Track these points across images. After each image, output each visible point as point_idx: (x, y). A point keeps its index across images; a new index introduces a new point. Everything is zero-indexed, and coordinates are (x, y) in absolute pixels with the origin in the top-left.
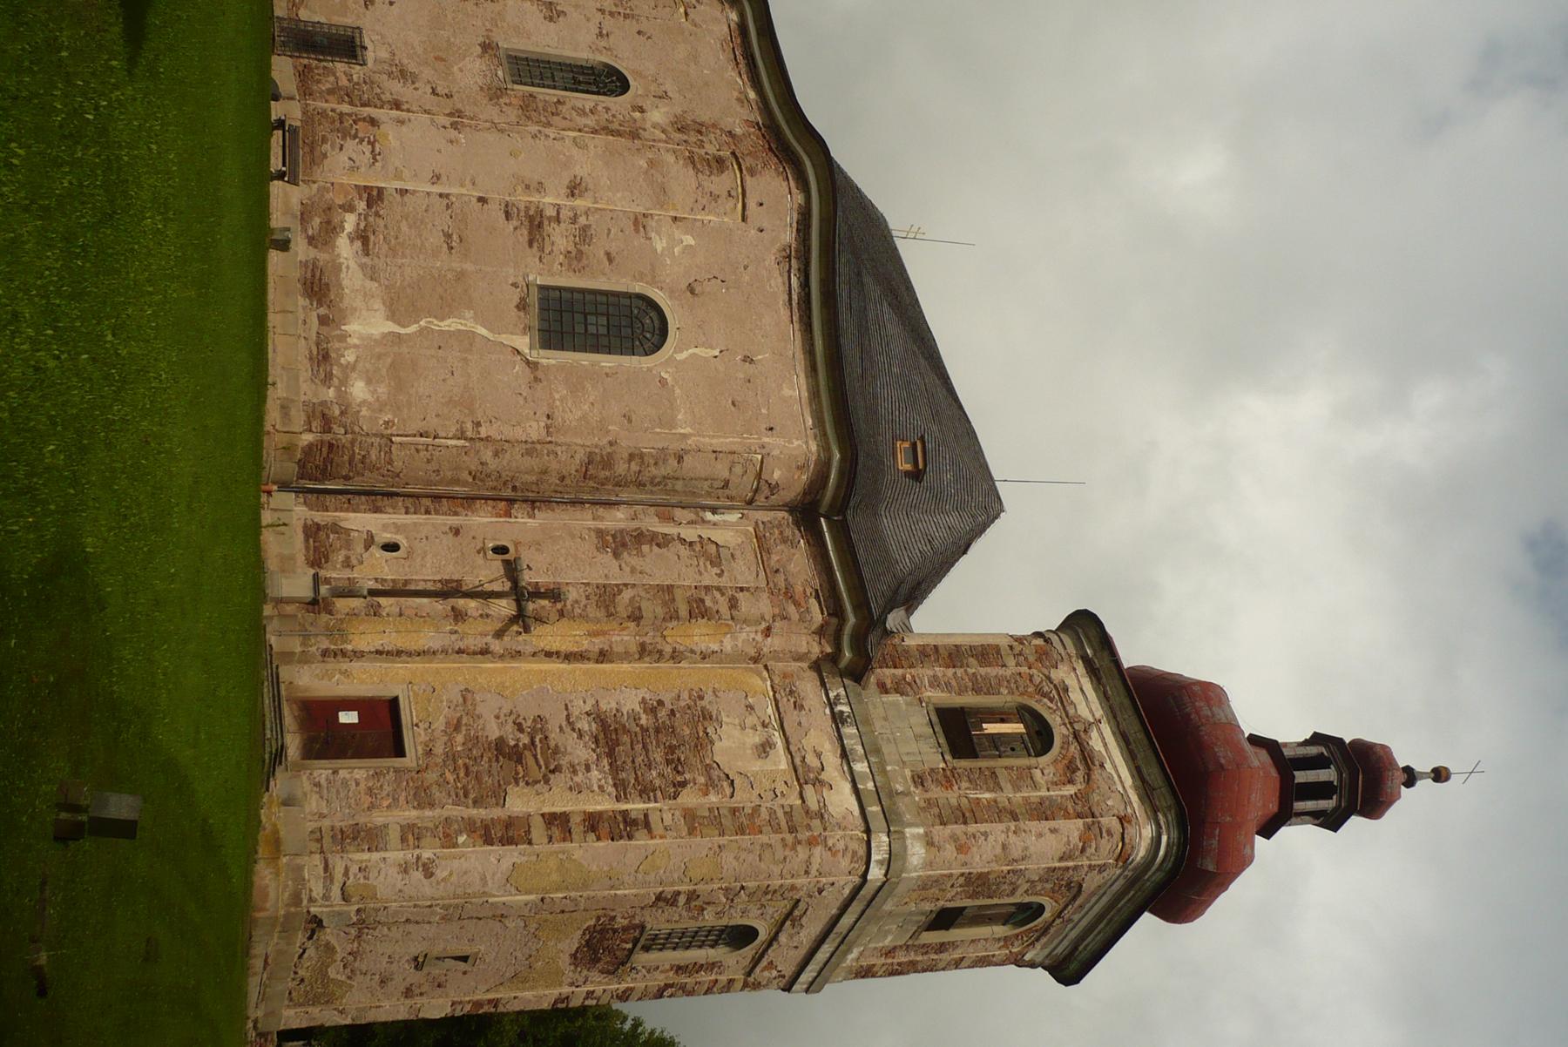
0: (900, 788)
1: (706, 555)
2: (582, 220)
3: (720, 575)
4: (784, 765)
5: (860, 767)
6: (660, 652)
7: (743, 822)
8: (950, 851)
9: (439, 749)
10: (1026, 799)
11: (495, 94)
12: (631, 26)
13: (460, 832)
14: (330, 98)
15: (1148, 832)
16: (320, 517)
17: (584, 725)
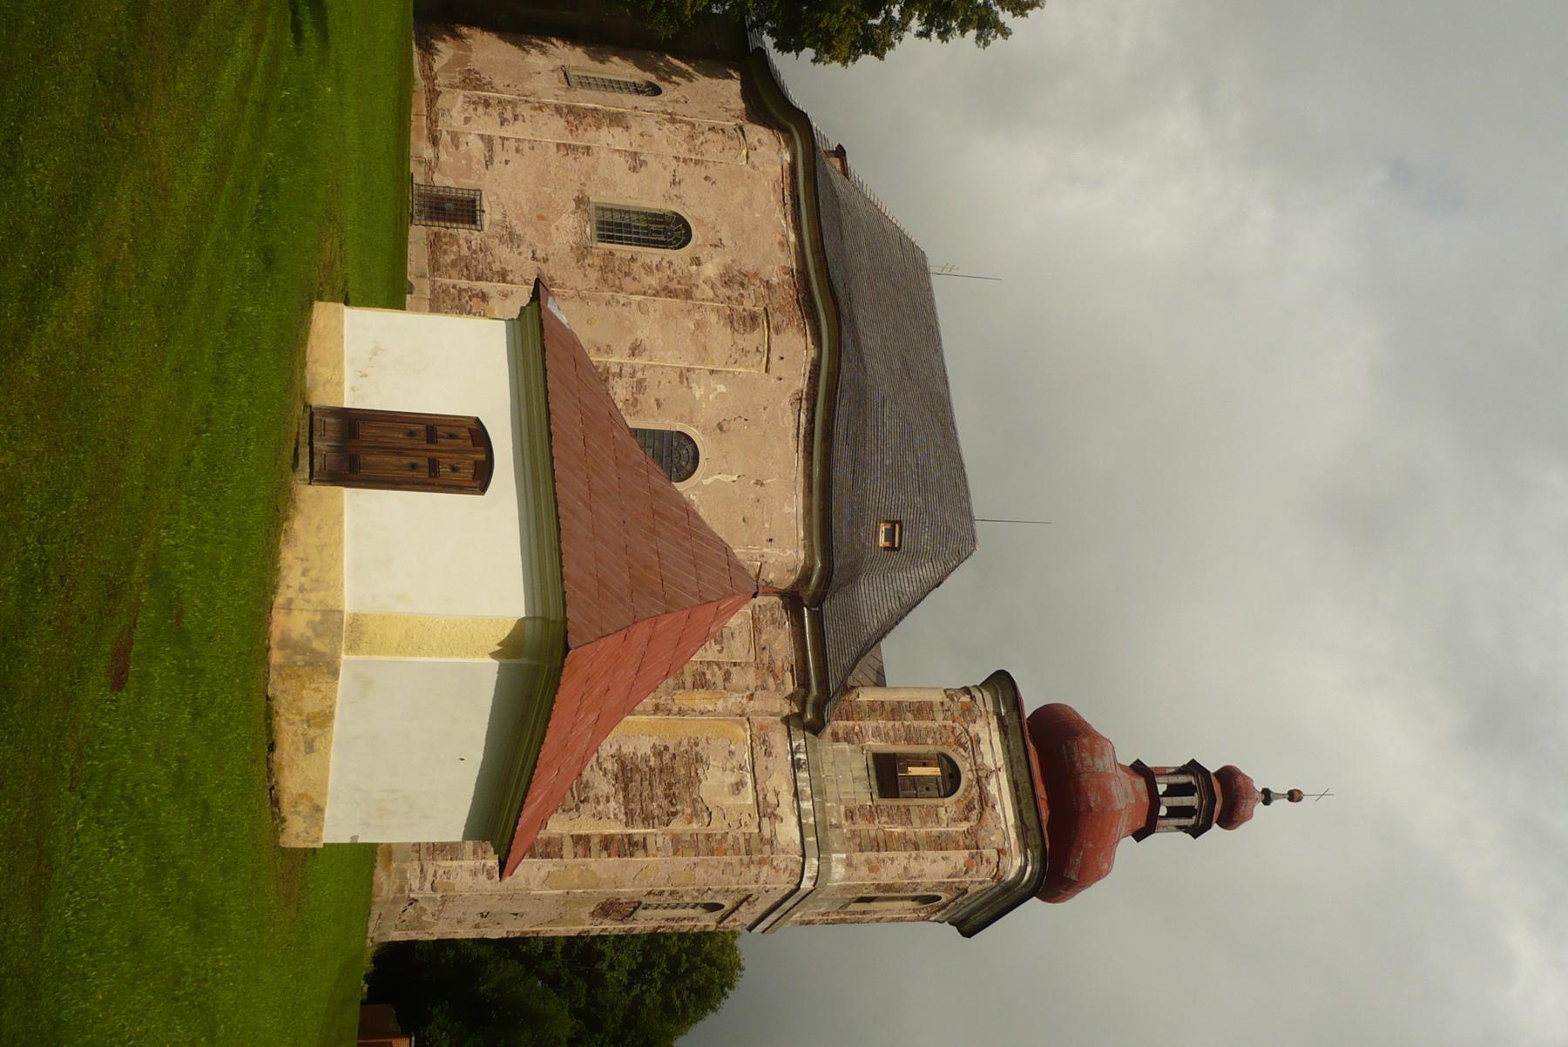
0: (834, 821)
2: (639, 375)
4: (750, 801)
5: (806, 805)
7: (711, 845)
8: (864, 870)
10: (928, 835)
11: (581, 252)
12: (701, 172)
14: (453, 272)
15: (1018, 862)
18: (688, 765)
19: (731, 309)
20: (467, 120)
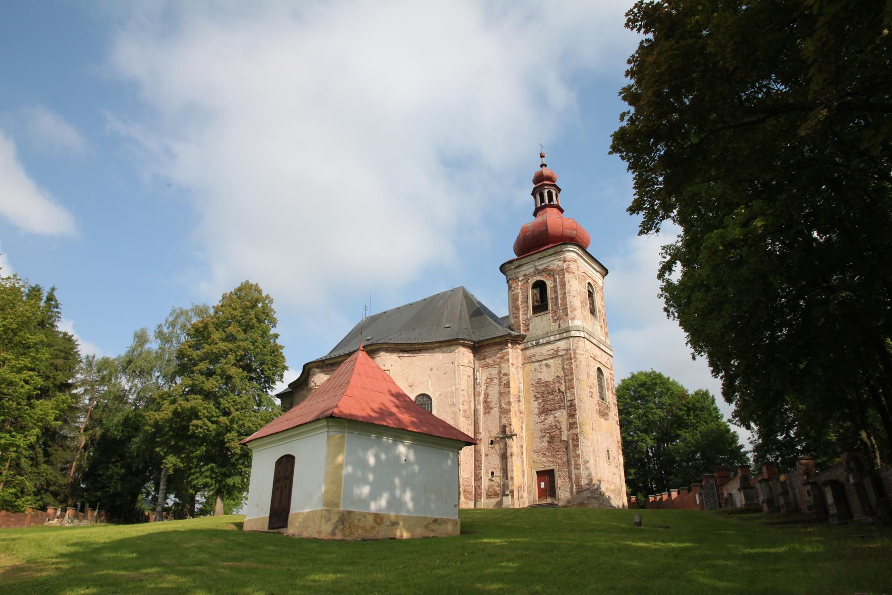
4: (552, 361)
5: (552, 338)
16: (484, 495)
17: (542, 418)
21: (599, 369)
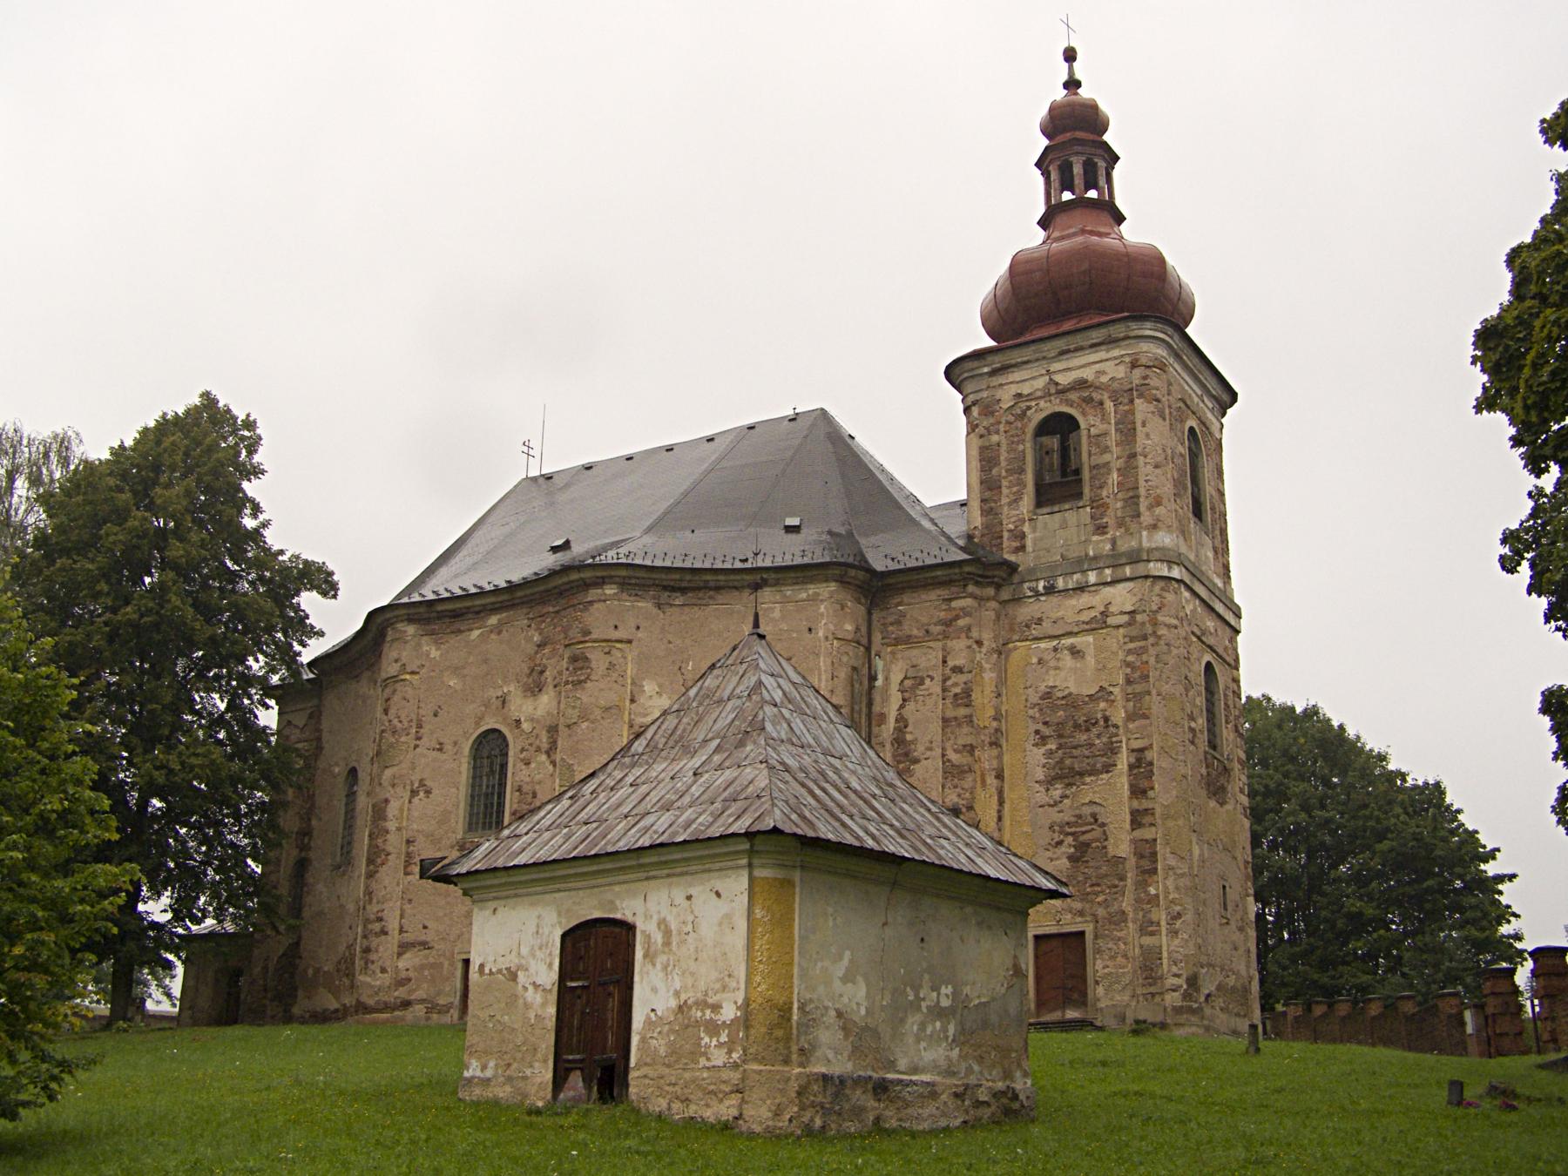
0: (1108, 547)
1: (914, 688)
3: (932, 679)
4: (1090, 639)
6: (997, 730)
7: (1137, 677)
9: (1078, 905)
13: (1146, 892)
17: (1057, 793)
18: (1054, 708)
19: (567, 683)
20: (383, 970)
21: (1209, 665)
